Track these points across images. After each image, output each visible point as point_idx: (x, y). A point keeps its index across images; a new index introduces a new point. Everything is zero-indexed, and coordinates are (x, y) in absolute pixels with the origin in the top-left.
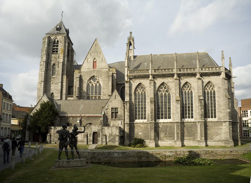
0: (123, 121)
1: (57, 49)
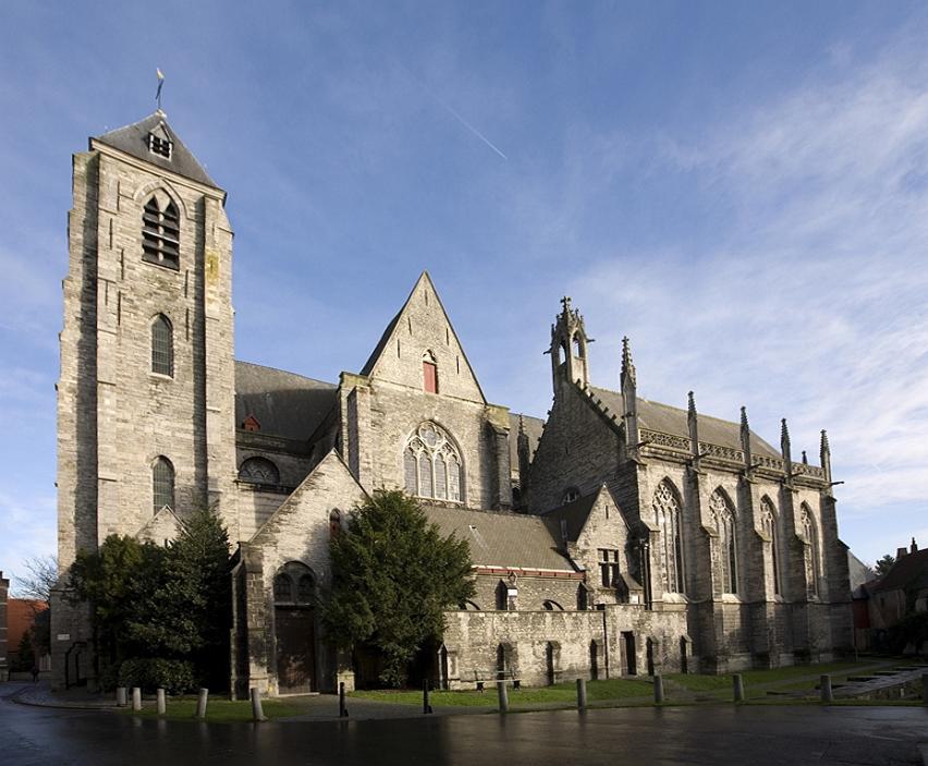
1: (176, 246)
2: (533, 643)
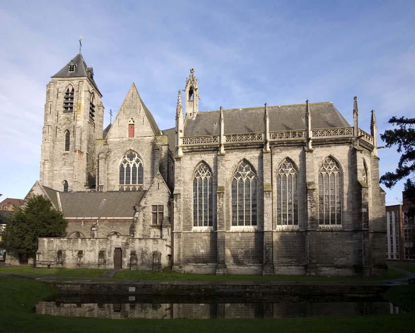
0: (170, 229)
1: (72, 103)
2: (72, 251)
